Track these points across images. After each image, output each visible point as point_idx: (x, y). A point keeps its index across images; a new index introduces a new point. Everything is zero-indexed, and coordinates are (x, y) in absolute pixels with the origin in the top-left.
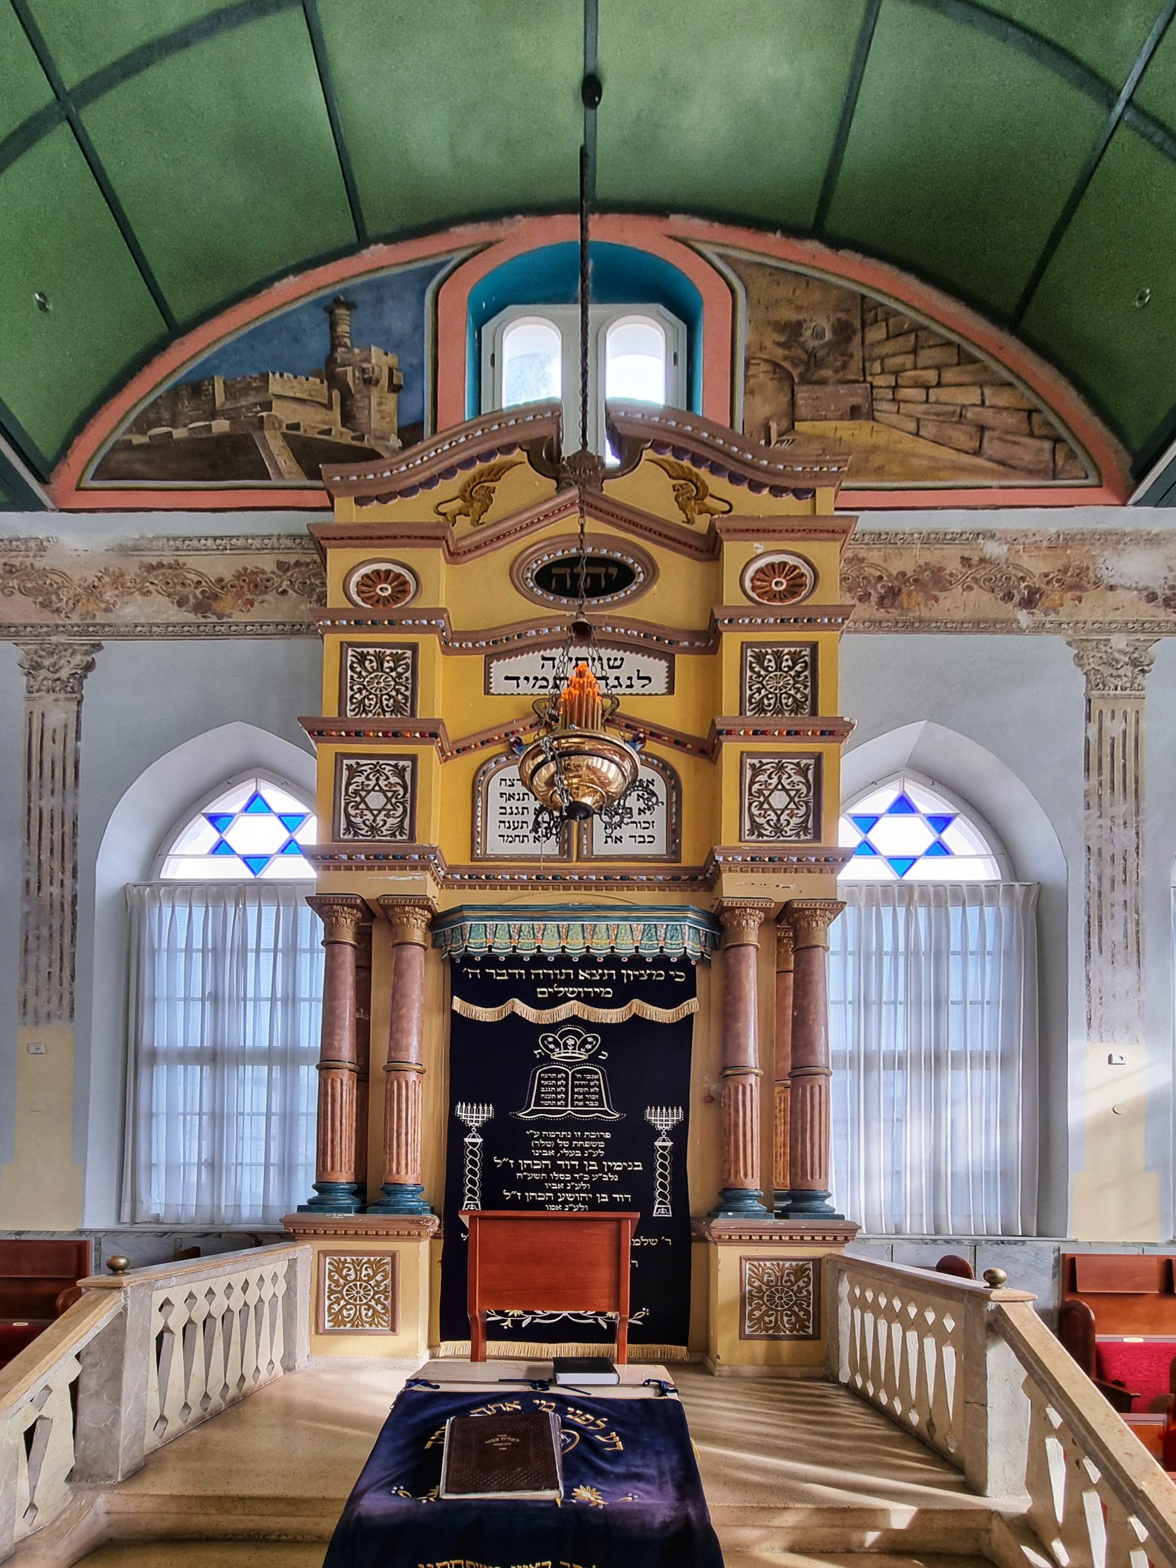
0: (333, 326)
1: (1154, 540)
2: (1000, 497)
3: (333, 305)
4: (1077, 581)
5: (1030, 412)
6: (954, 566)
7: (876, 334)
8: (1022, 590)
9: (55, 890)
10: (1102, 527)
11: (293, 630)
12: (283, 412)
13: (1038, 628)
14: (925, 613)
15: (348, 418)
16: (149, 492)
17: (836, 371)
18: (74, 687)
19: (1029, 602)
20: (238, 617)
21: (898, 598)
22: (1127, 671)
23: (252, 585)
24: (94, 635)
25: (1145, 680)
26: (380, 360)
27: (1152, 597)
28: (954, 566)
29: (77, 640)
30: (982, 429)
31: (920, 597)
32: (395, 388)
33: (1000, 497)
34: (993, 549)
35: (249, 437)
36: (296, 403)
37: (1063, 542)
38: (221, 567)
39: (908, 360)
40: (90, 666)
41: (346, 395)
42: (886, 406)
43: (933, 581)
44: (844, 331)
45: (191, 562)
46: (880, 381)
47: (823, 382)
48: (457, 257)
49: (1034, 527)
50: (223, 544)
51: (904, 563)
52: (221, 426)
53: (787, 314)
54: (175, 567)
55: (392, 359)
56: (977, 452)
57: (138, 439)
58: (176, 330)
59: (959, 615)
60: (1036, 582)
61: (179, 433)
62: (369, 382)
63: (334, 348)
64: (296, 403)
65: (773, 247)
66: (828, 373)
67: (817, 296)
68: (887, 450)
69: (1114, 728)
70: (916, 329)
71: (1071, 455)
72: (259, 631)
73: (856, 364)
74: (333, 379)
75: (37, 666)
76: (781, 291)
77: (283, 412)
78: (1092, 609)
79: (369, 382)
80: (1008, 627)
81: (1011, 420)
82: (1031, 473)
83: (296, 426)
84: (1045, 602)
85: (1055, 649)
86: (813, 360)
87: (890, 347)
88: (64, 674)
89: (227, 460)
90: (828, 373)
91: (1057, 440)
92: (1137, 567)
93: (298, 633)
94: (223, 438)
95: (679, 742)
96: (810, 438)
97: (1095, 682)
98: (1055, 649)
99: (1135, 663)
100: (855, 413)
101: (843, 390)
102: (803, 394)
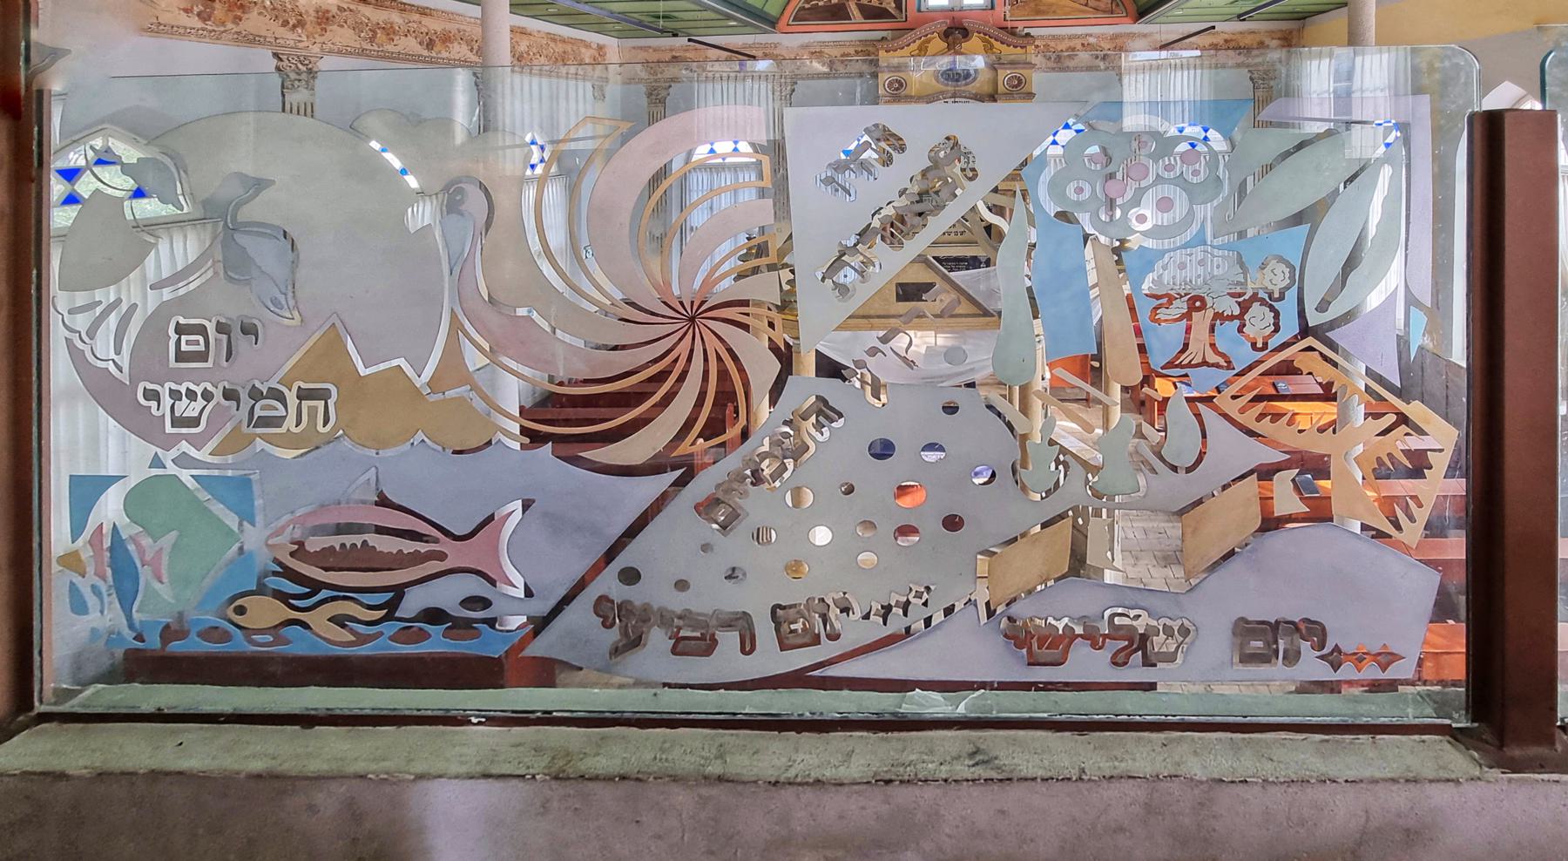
1: (1145, 36)
2: (1093, 21)
6: (1079, 47)
13: (1107, 69)
16: (812, 25)
21: (1059, 61)
34: (1092, 40)
37: (1115, 37)
38: (836, 52)
45: (826, 50)
50: (837, 44)
51: (1063, 46)
80: (1097, 68)
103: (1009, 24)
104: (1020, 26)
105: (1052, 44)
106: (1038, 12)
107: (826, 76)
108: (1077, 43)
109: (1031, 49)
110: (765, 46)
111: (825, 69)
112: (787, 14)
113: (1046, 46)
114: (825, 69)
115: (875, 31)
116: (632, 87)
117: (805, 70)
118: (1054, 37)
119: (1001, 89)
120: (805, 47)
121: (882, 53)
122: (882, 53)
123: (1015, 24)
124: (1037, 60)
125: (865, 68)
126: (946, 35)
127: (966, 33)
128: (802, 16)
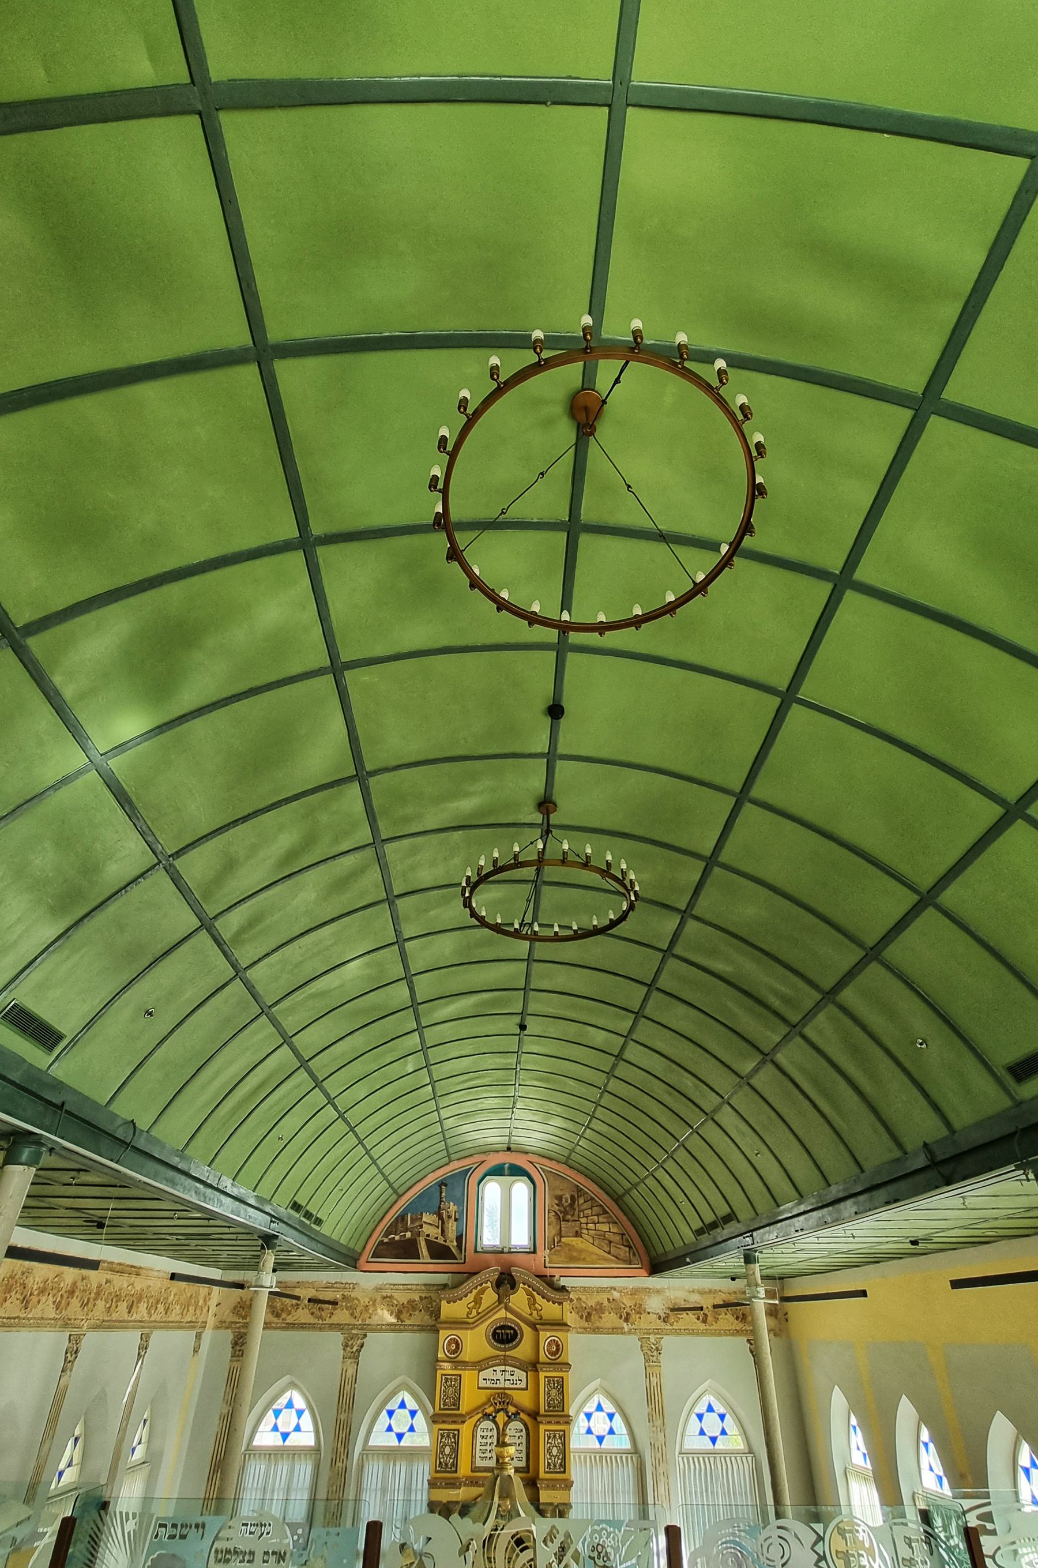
0: (441, 1193)
1: (658, 1292)
2: (616, 1272)
3: (442, 1184)
4: (640, 1310)
5: (623, 1234)
6: (606, 1303)
7: (581, 1201)
8: (624, 1315)
9: (340, 1464)
10: (645, 1286)
11: (422, 1328)
12: (427, 1230)
13: (630, 1332)
14: (598, 1324)
15: (443, 1231)
17: (573, 1215)
18: (356, 1356)
19: (627, 1320)
20: (407, 1322)
22: (655, 1353)
23: (412, 1305)
24: (366, 1328)
25: (661, 1358)
26: (453, 1208)
27: (660, 1318)
28: (606, 1303)
29: (360, 1332)
30: (610, 1242)
31: (597, 1317)
32: (456, 1220)
33: (616, 1272)
34: (616, 1295)
35: (415, 1240)
36: (430, 1229)
37: (635, 1292)
38: (402, 1298)
39: (589, 1212)
40: (362, 1346)
41: (443, 1223)
42: (585, 1231)
43: (600, 1309)
44: (572, 1198)
46: (584, 1220)
47: (568, 1221)
48: (475, 1166)
49: (627, 1285)
52: (408, 1235)
53: (560, 1193)
54: (391, 1297)
55: (456, 1207)
56: (609, 1253)
57: (386, 1240)
58: (400, 1196)
59: (609, 1325)
60: (628, 1310)
61: (397, 1238)
62: (449, 1217)
63: (441, 1201)
64: (430, 1229)
65: (553, 1164)
66: (569, 1217)
67: (565, 1185)
68: (587, 1251)
69: (654, 1380)
70: (592, 1199)
71: (634, 1254)
72: (412, 1329)
73: (576, 1212)
74: (440, 1217)
75: (347, 1346)
76: (557, 1183)
77: (427, 1230)
78: (644, 1323)
79: (449, 1217)
81: (618, 1238)
82: (624, 1261)
83: (428, 1235)
84: (631, 1320)
85: (633, 1340)
86: (565, 1213)
87: (585, 1206)
88: (354, 1349)
89: (407, 1250)
90: (569, 1217)
91: (630, 1247)
92: (655, 1304)
93: (422, 1330)
94: (409, 1239)
95: (529, 1415)
96: (566, 1244)
97: (647, 1361)
98: (633, 1340)
99: (657, 1349)
100: (577, 1234)
101: (574, 1223)
102: (563, 1224)
103: (549, 1272)
104: (557, 1273)
105: (583, 1298)
106: (572, 1259)
107: (392, 1328)
108: (603, 1298)
109: (566, 1305)
110: (345, 1286)
111: (393, 1320)
112: (369, 1247)
113: (579, 1299)
114: (393, 1320)
115: (436, 1274)
116: (222, 1331)
117: (375, 1320)
118: (585, 1290)
119: (543, 1358)
120: (378, 1289)
121: (444, 1303)
122: (444, 1303)
123: (553, 1272)
124: (571, 1318)
125: (428, 1320)
126: (498, 1285)
127: (513, 1286)
128: (379, 1253)
